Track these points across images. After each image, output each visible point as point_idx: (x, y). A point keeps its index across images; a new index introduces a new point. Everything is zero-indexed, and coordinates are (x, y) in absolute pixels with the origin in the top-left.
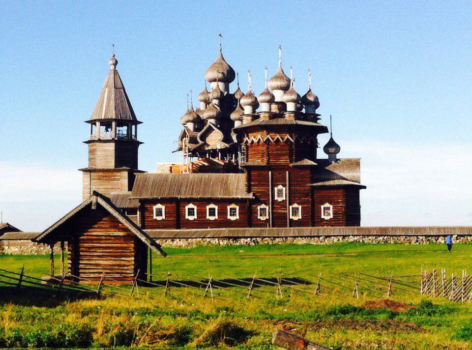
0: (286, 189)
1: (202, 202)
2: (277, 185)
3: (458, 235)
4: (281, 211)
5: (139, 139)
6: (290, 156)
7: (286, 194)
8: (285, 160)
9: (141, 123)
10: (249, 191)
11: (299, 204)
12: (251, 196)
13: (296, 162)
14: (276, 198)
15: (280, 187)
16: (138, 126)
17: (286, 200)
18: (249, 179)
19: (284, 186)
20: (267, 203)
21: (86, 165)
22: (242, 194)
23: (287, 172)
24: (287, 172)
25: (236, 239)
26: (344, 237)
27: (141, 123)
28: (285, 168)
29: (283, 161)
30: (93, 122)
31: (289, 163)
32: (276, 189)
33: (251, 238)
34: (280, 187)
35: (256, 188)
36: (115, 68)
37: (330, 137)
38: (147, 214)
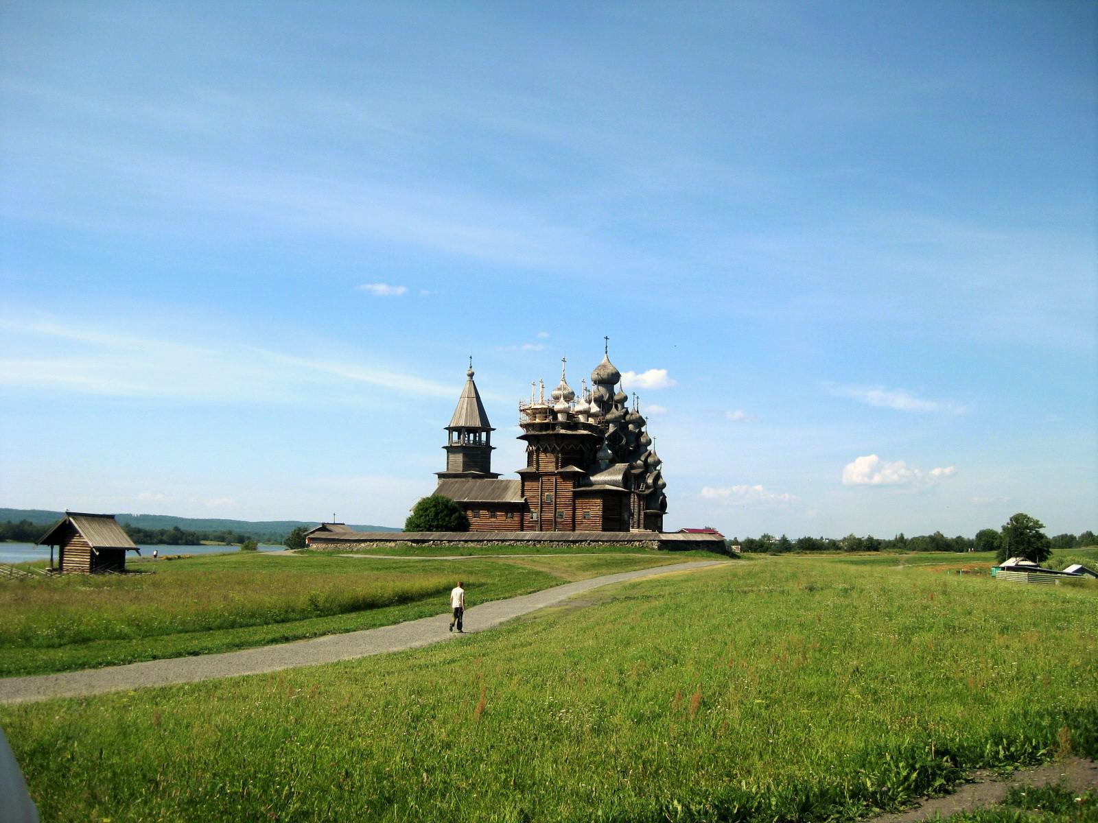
3: (591, 541)
5: (492, 444)
6: (557, 463)
9: (494, 429)
10: (523, 495)
13: (562, 467)
16: (492, 432)
18: (523, 486)
21: (443, 469)
22: (518, 499)
25: (424, 541)
26: (503, 541)
27: (494, 429)
28: (552, 474)
29: (551, 468)
30: (451, 430)
33: (434, 541)
36: (472, 378)
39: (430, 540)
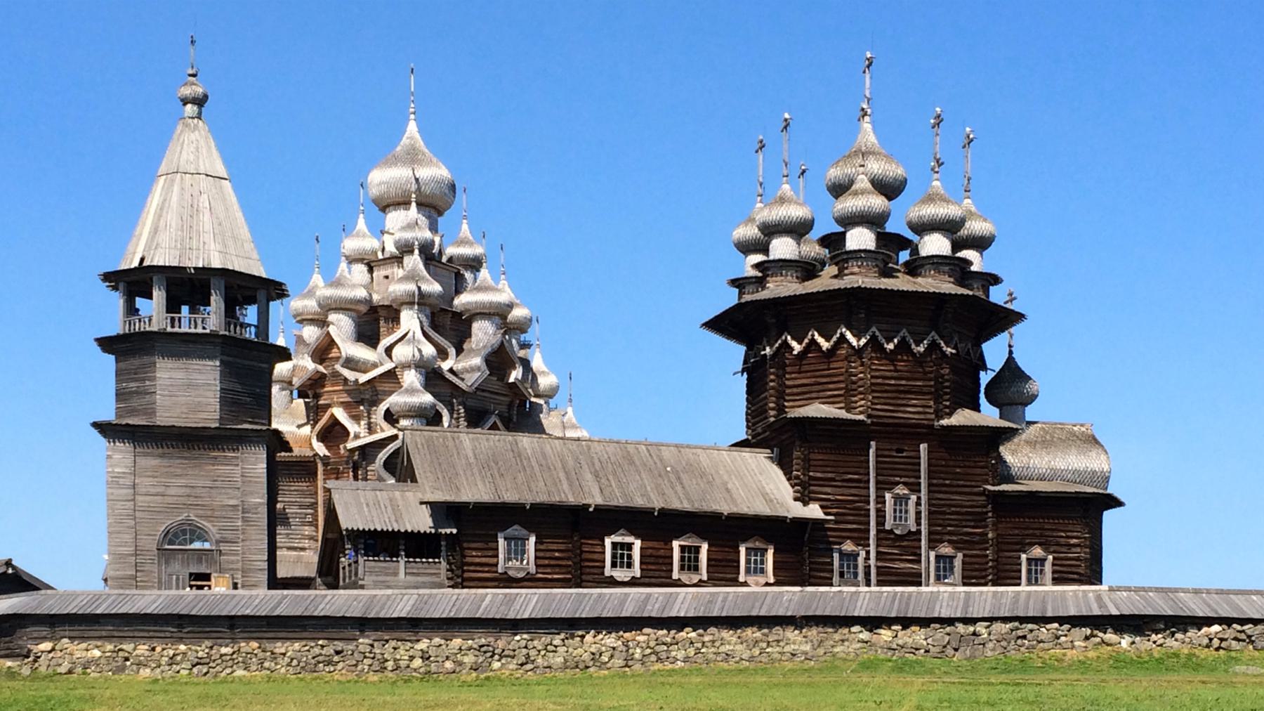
0: (919, 498)
1: (658, 525)
2: (891, 486)
4: (902, 565)
7: (918, 514)
8: (920, 409)
11: (957, 545)
12: (814, 511)
14: (887, 527)
15: (901, 490)
17: (919, 532)
19: (915, 488)
20: (862, 540)
23: (923, 447)
24: (923, 447)
31: (933, 416)
32: (888, 496)
33: (1227, 621)
34: (901, 490)
35: (828, 490)
37: (1007, 356)
38: (474, 557)
39: (1209, 621)
